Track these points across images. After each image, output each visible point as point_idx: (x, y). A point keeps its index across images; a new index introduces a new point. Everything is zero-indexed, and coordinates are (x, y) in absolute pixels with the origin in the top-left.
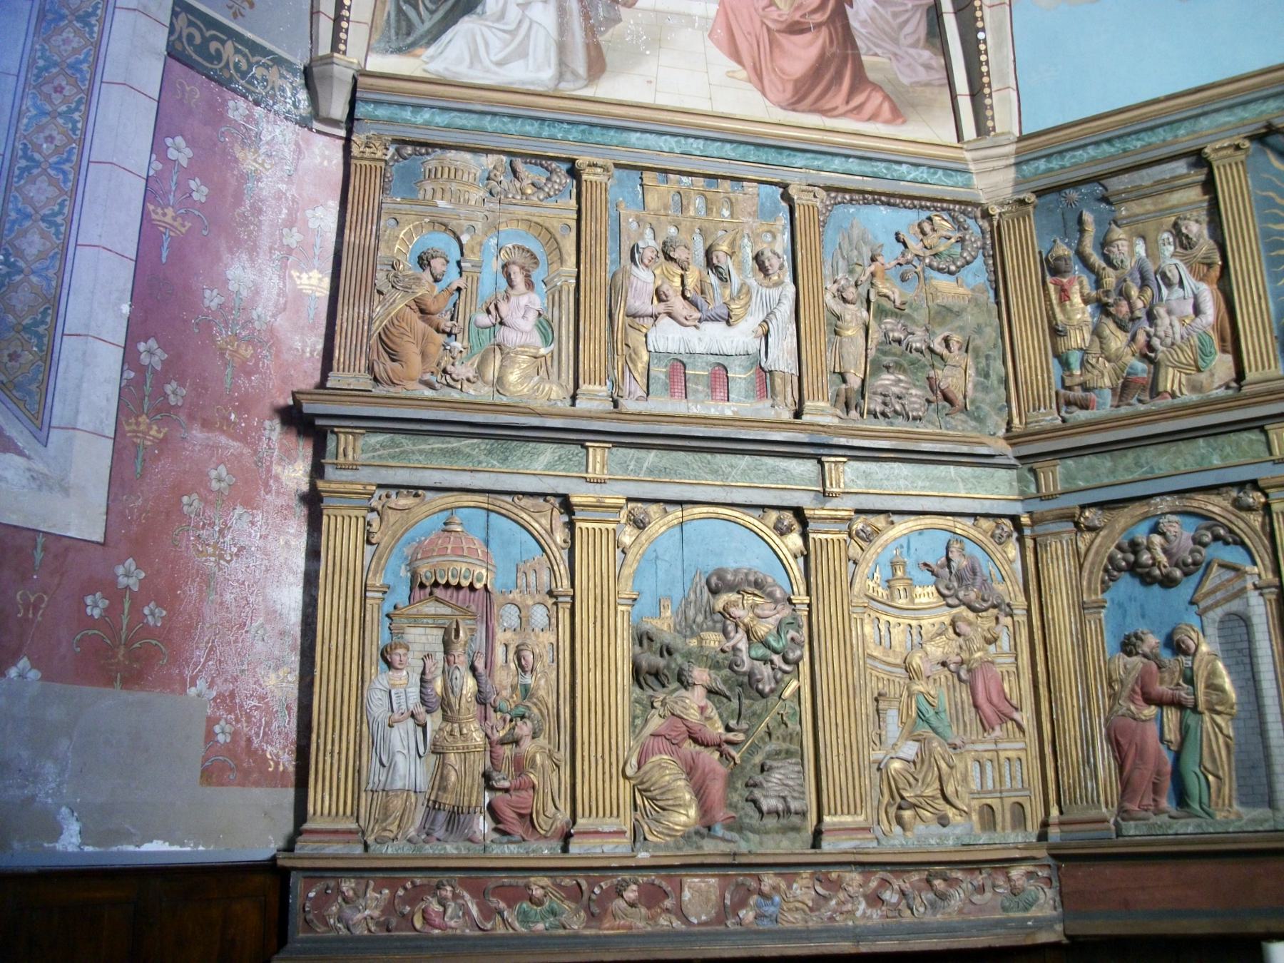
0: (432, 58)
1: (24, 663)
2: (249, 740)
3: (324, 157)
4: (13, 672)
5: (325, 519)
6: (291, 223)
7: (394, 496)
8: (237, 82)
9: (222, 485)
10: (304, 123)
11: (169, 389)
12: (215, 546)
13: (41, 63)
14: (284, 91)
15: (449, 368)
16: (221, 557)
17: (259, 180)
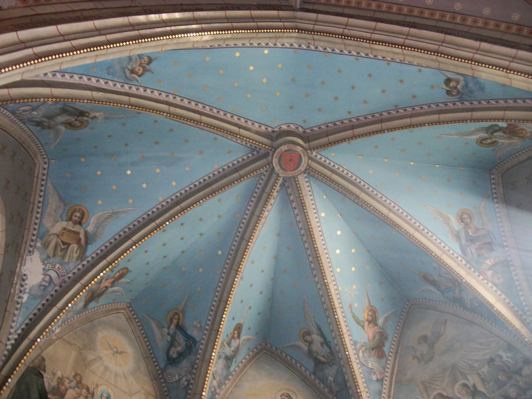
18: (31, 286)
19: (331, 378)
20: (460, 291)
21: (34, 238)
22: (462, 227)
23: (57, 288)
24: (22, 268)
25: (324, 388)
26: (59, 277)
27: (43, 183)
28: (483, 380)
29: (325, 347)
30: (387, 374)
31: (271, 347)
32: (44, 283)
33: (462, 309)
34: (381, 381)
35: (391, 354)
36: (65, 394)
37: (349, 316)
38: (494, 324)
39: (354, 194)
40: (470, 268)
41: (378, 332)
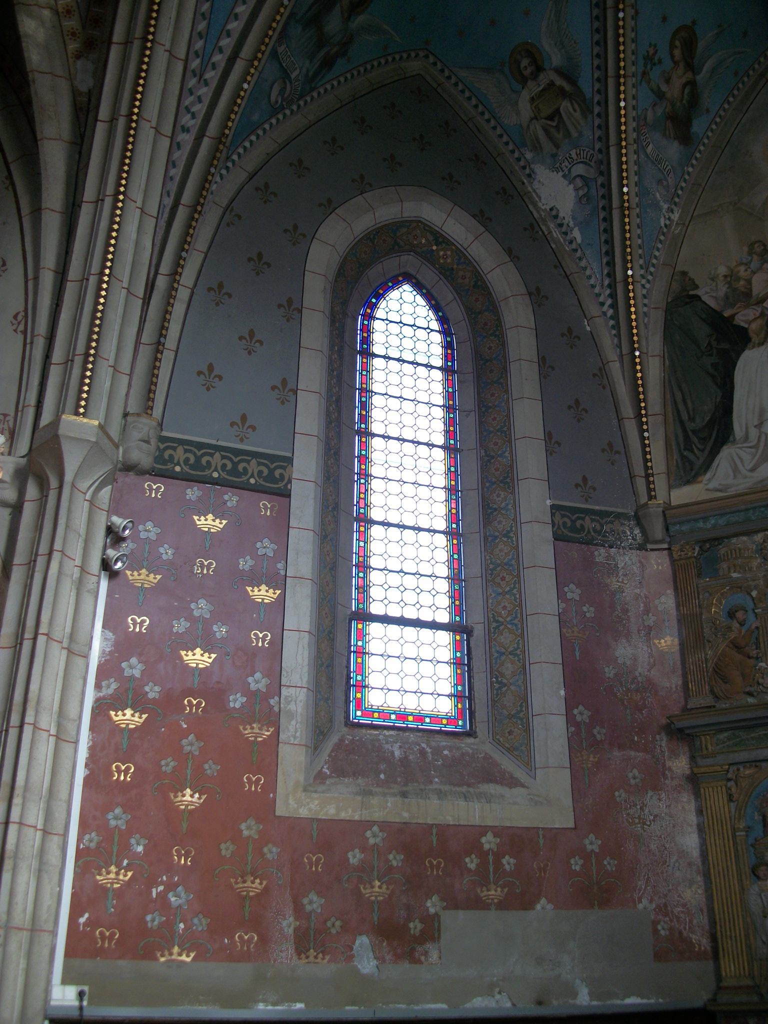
0: (710, 480)
1: (543, 901)
2: (681, 933)
3: (658, 564)
4: (538, 907)
5: (702, 791)
6: (647, 611)
7: (742, 769)
8: (597, 539)
9: (637, 780)
10: (642, 547)
11: (595, 731)
12: (639, 818)
13: (491, 566)
14: (625, 533)
15: (761, 681)
16: (644, 824)
17: (623, 592)
18: (570, 213)
21: (516, 155)
23: (600, 180)
24: (540, 204)
26: (589, 165)
27: (453, 80)
32: (581, 193)
36: (751, 290)
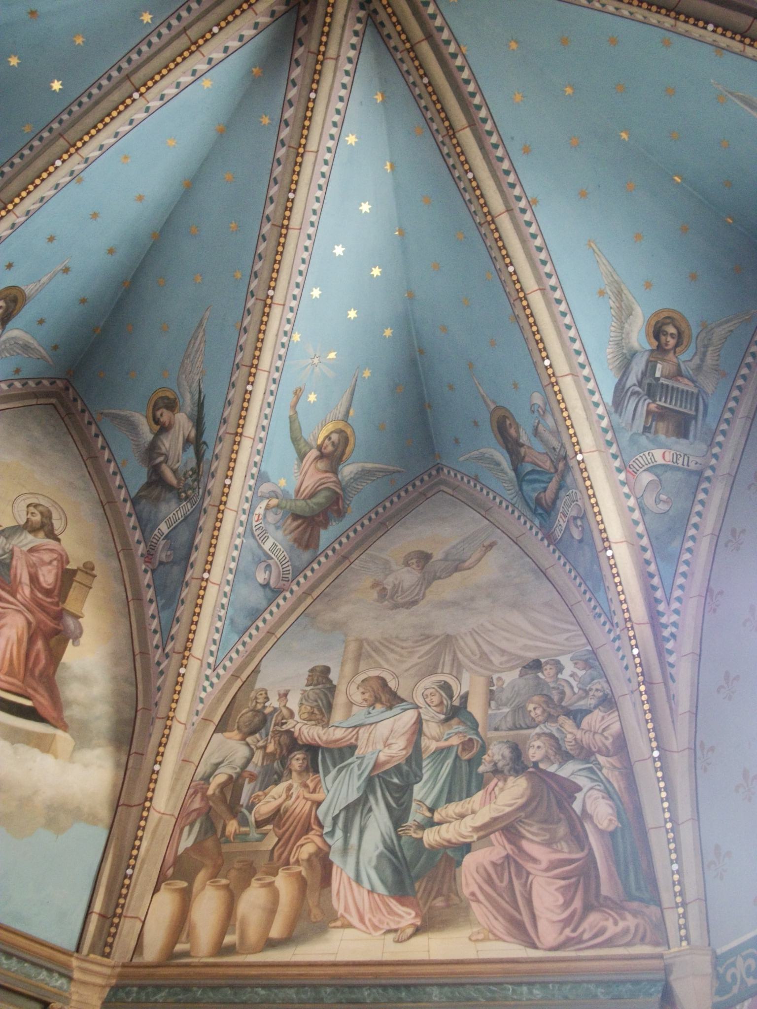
19: (164, 528)
20: (560, 487)
22: (648, 347)
25: (139, 542)
28: (491, 695)
29: (191, 450)
30: (295, 588)
31: (75, 400)
33: (540, 536)
34: (273, 592)
35: (330, 553)
37: (282, 413)
38: (588, 596)
39: (447, 118)
40: (609, 444)
41: (328, 489)
